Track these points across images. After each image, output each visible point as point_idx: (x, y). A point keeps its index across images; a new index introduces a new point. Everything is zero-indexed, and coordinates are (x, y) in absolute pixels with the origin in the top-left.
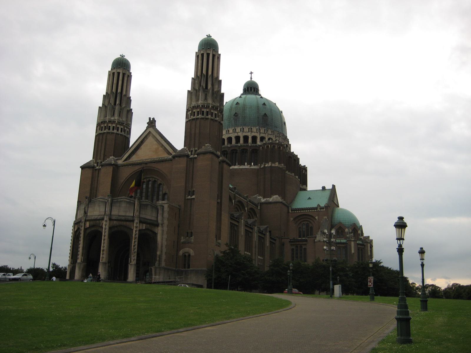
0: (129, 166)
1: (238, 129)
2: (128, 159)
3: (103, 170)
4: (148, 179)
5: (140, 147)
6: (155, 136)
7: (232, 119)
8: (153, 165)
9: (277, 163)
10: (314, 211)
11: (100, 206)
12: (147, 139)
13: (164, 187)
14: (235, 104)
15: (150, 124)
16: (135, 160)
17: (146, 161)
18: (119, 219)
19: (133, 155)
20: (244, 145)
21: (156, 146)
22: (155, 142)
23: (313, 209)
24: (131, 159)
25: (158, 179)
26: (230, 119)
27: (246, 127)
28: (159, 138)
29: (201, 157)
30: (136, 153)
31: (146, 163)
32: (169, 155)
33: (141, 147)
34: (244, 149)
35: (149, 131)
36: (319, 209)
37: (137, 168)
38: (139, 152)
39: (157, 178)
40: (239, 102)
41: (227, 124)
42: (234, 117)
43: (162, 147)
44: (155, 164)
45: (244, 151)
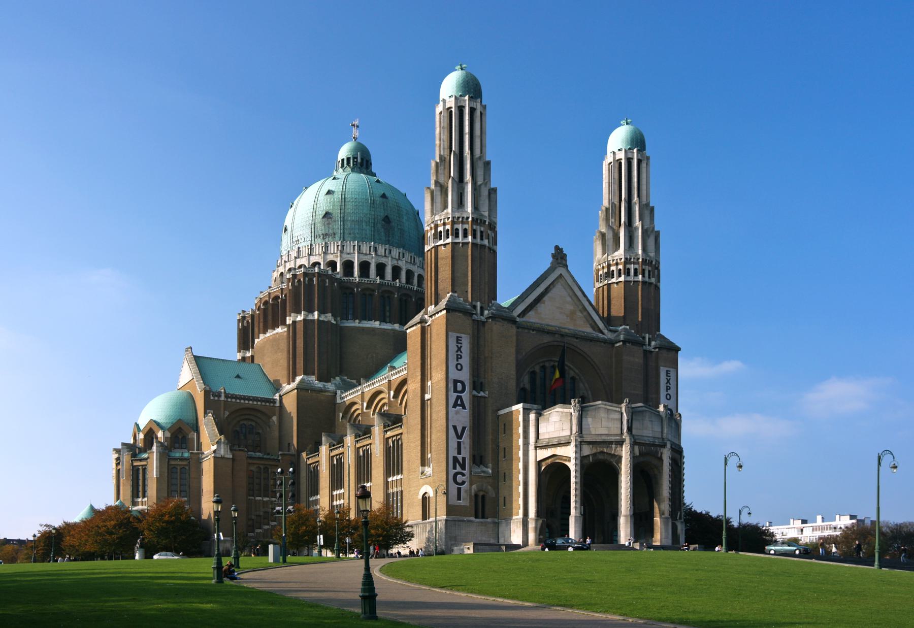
0: (531, 332)
1: (395, 252)
2: (521, 316)
3: (497, 328)
4: (552, 363)
5: (542, 298)
6: (572, 287)
7: (379, 226)
8: (575, 342)
9: (316, 313)
10: (261, 405)
11: (652, 421)
12: (554, 287)
13: (581, 385)
14: (378, 195)
15: (559, 258)
16: (534, 321)
17: (550, 328)
18: (598, 440)
19: (530, 311)
20: (407, 287)
21: (572, 308)
22: (569, 299)
23: (238, 398)
24: (528, 315)
25: (570, 368)
26: (374, 224)
27: (407, 252)
28: (579, 294)
29: (664, 353)
30: (535, 308)
31: (562, 335)
32: (594, 329)
33: (544, 299)
34: (368, 289)
35: (559, 274)
36: (223, 398)
37: (546, 339)
38: (541, 307)
39: (572, 366)
40: (387, 194)
41: (368, 232)
42: (383, 222)
43: (581, 311)
44: (577, 340)
45: (367, 292)
